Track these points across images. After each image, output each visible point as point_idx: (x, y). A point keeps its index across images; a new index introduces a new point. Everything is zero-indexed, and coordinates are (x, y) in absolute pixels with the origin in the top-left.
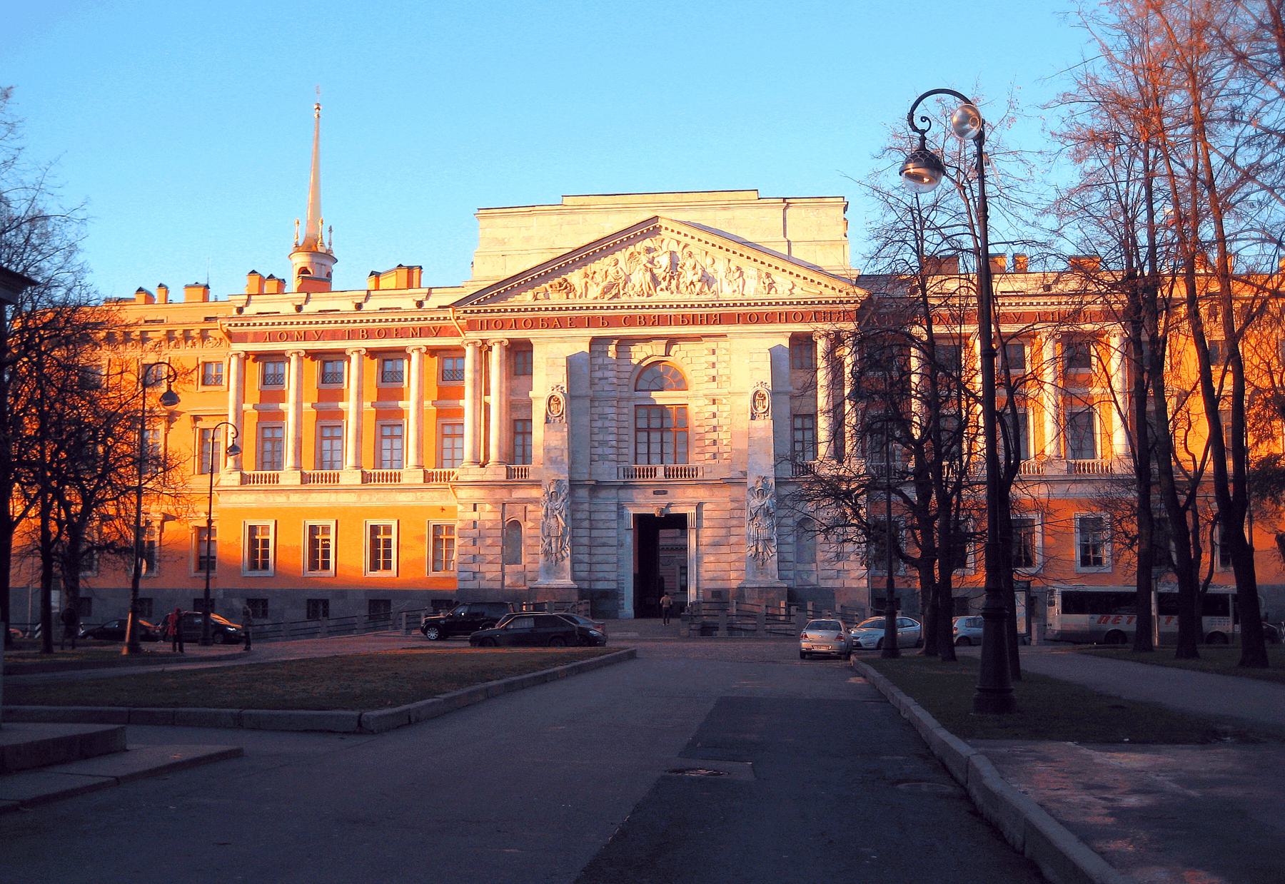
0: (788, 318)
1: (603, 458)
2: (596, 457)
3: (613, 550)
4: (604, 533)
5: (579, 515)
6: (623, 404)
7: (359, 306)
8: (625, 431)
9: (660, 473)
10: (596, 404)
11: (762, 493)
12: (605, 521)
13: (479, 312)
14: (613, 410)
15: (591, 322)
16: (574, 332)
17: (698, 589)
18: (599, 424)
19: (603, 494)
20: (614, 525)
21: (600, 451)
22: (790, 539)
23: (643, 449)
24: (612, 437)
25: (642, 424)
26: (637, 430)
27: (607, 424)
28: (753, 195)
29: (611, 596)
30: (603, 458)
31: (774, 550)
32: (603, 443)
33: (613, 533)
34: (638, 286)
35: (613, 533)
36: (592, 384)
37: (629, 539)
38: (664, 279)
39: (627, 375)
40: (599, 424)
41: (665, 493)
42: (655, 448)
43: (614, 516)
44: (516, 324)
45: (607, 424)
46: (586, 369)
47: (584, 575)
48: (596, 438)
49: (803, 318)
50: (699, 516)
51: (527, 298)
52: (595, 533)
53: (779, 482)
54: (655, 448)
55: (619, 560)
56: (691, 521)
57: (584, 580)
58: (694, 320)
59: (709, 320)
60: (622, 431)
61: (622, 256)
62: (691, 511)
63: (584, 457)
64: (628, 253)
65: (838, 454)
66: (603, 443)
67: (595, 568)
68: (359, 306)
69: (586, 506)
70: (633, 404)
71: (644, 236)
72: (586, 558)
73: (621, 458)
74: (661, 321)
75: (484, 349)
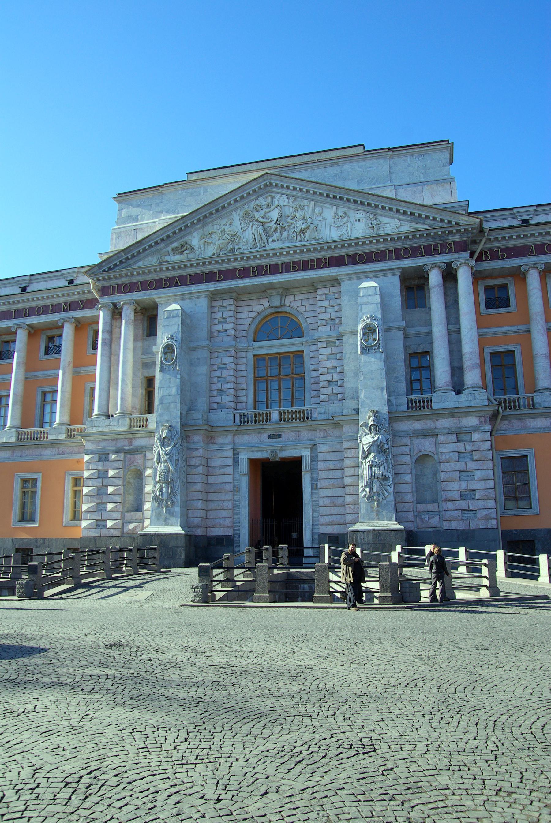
0: (398, 254)
1: (222, 406)
2: (215, 406)
3: (229, 496)
4: (220, 479)
5: (193, 462)
6: (243, 354)
7: (24, 289)
8: (244, 380)
9: (275, 416)
10: (216, 355)
11: (375, 428)
12: (222, 467)
13: (110, 278)
14: (231, 360)
15: (210, 277)
16: (193, 288)
17: (313, 534)
18: (218, 374)
19: (220, 440)
20: (230, 470)
21: (218, 399)
22: (408, 478)
23: (262, 397)
24: (230, 385)
25: (262, 373)
26: (256, 379)
27: (225, 373)
28: (360, 150)
29: (227, 542)
30: (222, 406)
31: (390, 489)
32: (223, 392)
33: (229, 479)
34: (251, 240)
35: (229, 479)
36: (211, 336)
37: (244, 483)
38: (276, 230)
39: (246, 327)
40: (218, 374)
41: (280, 436)
42: (274, 396)
43: (230, 462)
44: (144, 286)
45: (225, 373)
46: (204, 323)
47: (196, 521)
48: (214, 387)
49: (415, 252)
50: (314, 459)
51: (151, 261)
52: (211, 480)
53: (393, 417)
54: (274, 396)
55: (234, 507)
56: (305, 465)
57: (197, 526)
58: (305, 266)
59: (320, 264)
60: (240, 380)
61: (236, 217)
62: (305, 454)
63: (202, 403)
64: (241, 214)
65: (458, 387)
66: (223, 392)
67: (212, 514)
68: (24, 289)
69: (200, 452)
70: (250, 355)
71: (257, 193)
72: (200, 504)
73: (239, 406)
74: (275, 269)
75: (116, 312)
